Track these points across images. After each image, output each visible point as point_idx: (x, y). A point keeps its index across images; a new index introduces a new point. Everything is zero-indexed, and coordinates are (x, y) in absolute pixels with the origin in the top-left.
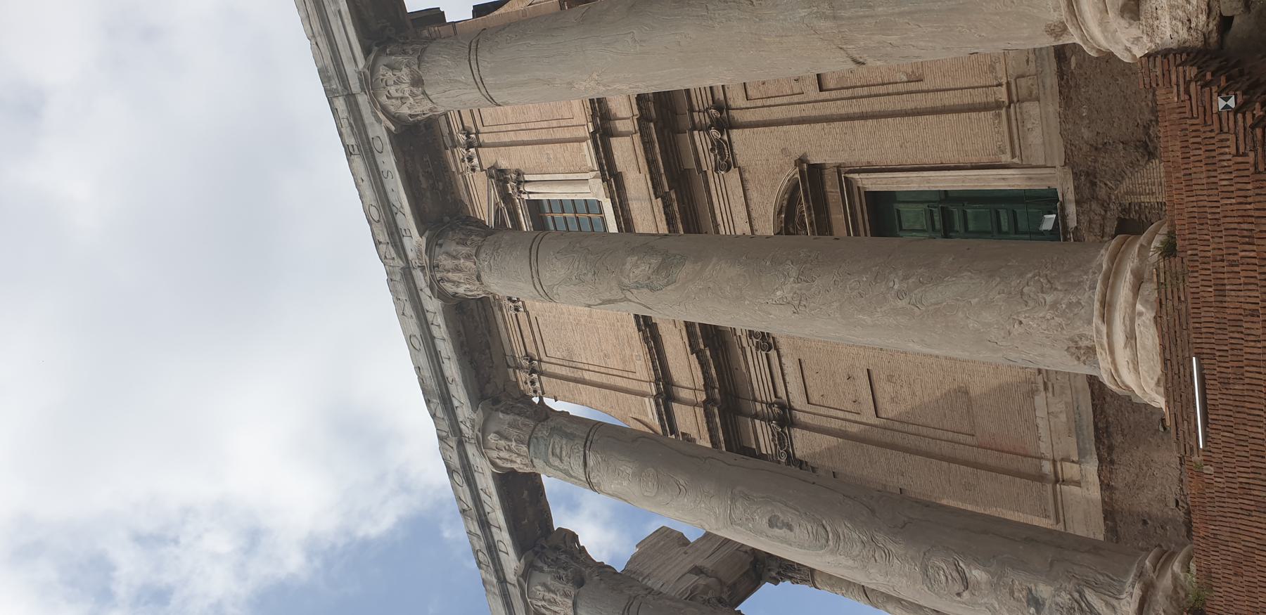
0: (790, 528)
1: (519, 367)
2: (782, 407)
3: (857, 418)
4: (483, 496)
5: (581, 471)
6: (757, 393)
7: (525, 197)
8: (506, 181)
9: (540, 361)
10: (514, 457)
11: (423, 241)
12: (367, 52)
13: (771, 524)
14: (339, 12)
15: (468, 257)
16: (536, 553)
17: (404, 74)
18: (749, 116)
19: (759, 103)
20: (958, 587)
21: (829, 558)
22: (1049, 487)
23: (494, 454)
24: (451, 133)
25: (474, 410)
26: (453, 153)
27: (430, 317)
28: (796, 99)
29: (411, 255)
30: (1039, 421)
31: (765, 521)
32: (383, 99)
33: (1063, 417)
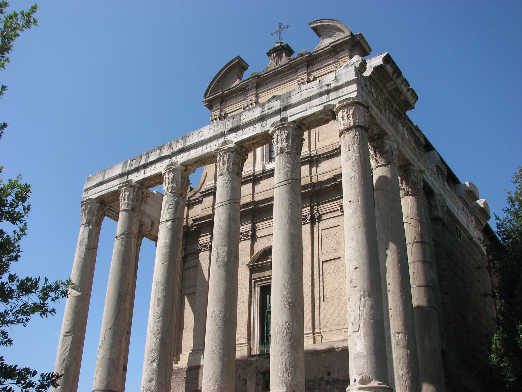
0: (158, 306)
1: (221, 111)
5: (165, 219)
10: (167, 185)
11: (232, 145)
12: (294, 122)
13: (158, 299)
14: (307, 110)
15: (228, 168)
16: (139, 187)
17: (284, 144)
20: (151, 360)
21: (152, 320)
23: (166, 175)
24: (314, 71)
25: (181, 164)
26: (305, 73)
27: (209, 144)
31: (159, 297)
32: (277, 132)
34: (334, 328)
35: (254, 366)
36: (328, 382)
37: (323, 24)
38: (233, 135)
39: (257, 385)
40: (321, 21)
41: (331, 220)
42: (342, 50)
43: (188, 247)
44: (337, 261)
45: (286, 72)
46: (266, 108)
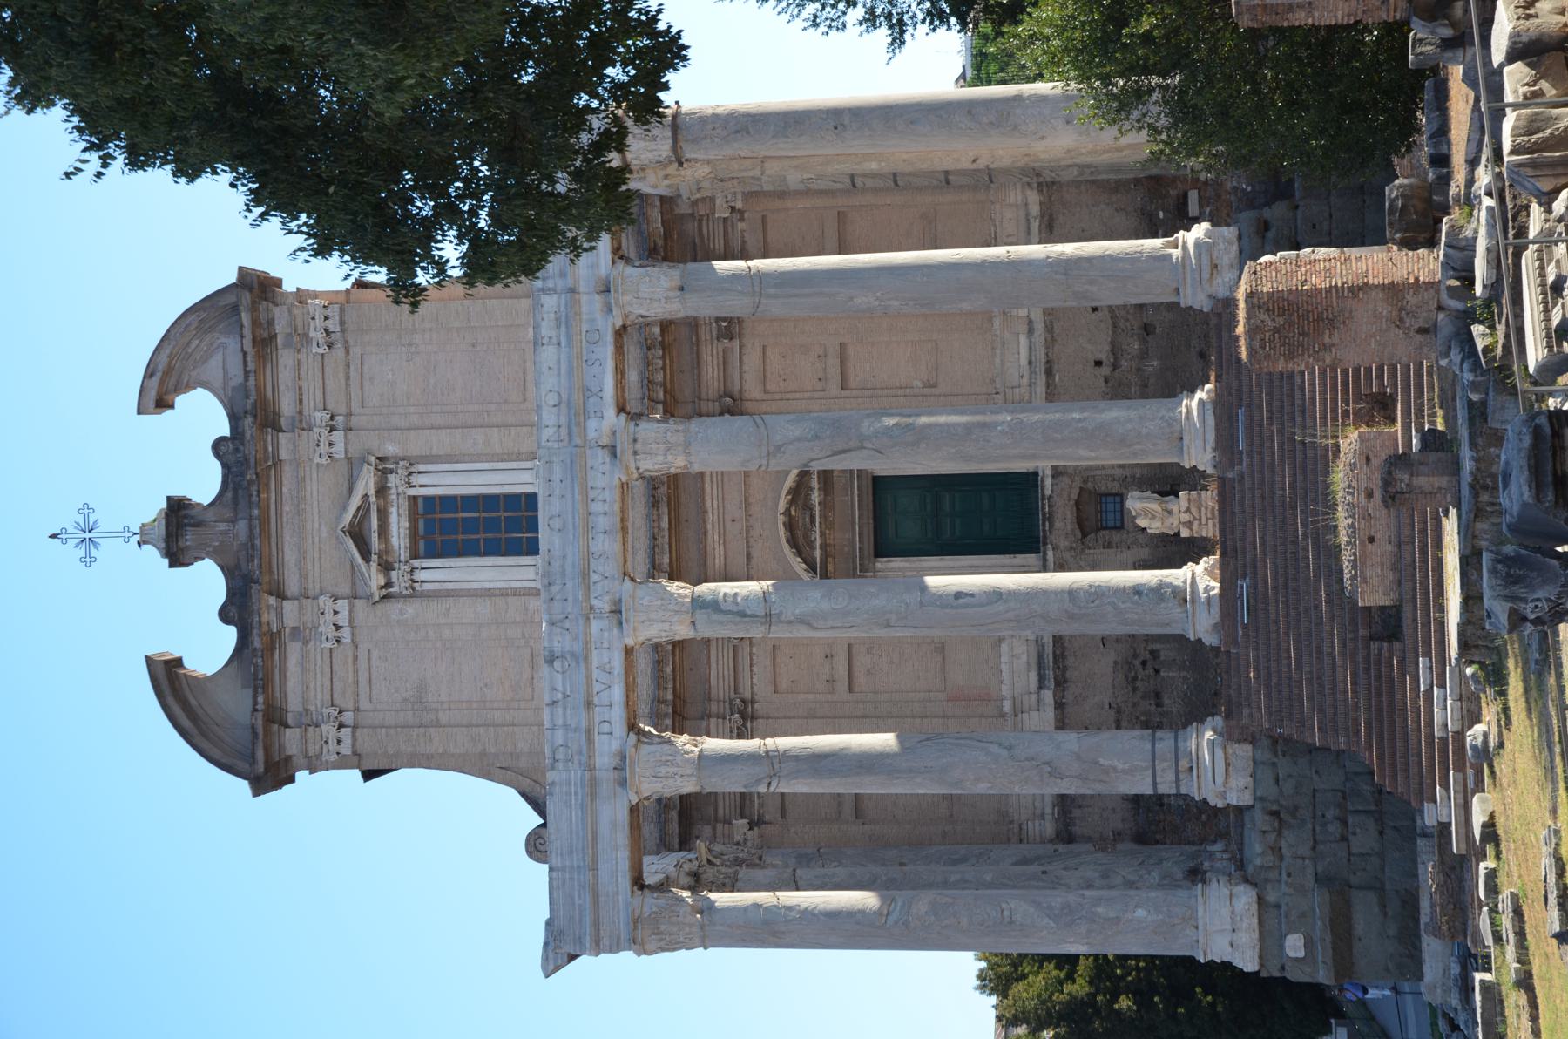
2: (743, 701)
3: (829, 697)
4: (596, 674)
6: (714, 692)
7: (412, 492)
8: (385, 472)
9: (356, 710)
12: (613, 262)
18: (763, 407)
19: (777, 396)
22: (1010, 721)
24: (300, 413)
27: (592, 494)
28: (817, 395)
29: (591, 435)
30: (1003, 667)
33: (1024, 658)
34: (998, 360)
35: (1067, 555)
36: (1115, 366)
37: (160, 367)
38: (592, 424)
39: (1109, 546)
40: (149, 374)
41: (746, 368)
42: (271, 322)
43: (721, 812)
44: (851, 351)
45: (268, 499)
46: (553, 333)
